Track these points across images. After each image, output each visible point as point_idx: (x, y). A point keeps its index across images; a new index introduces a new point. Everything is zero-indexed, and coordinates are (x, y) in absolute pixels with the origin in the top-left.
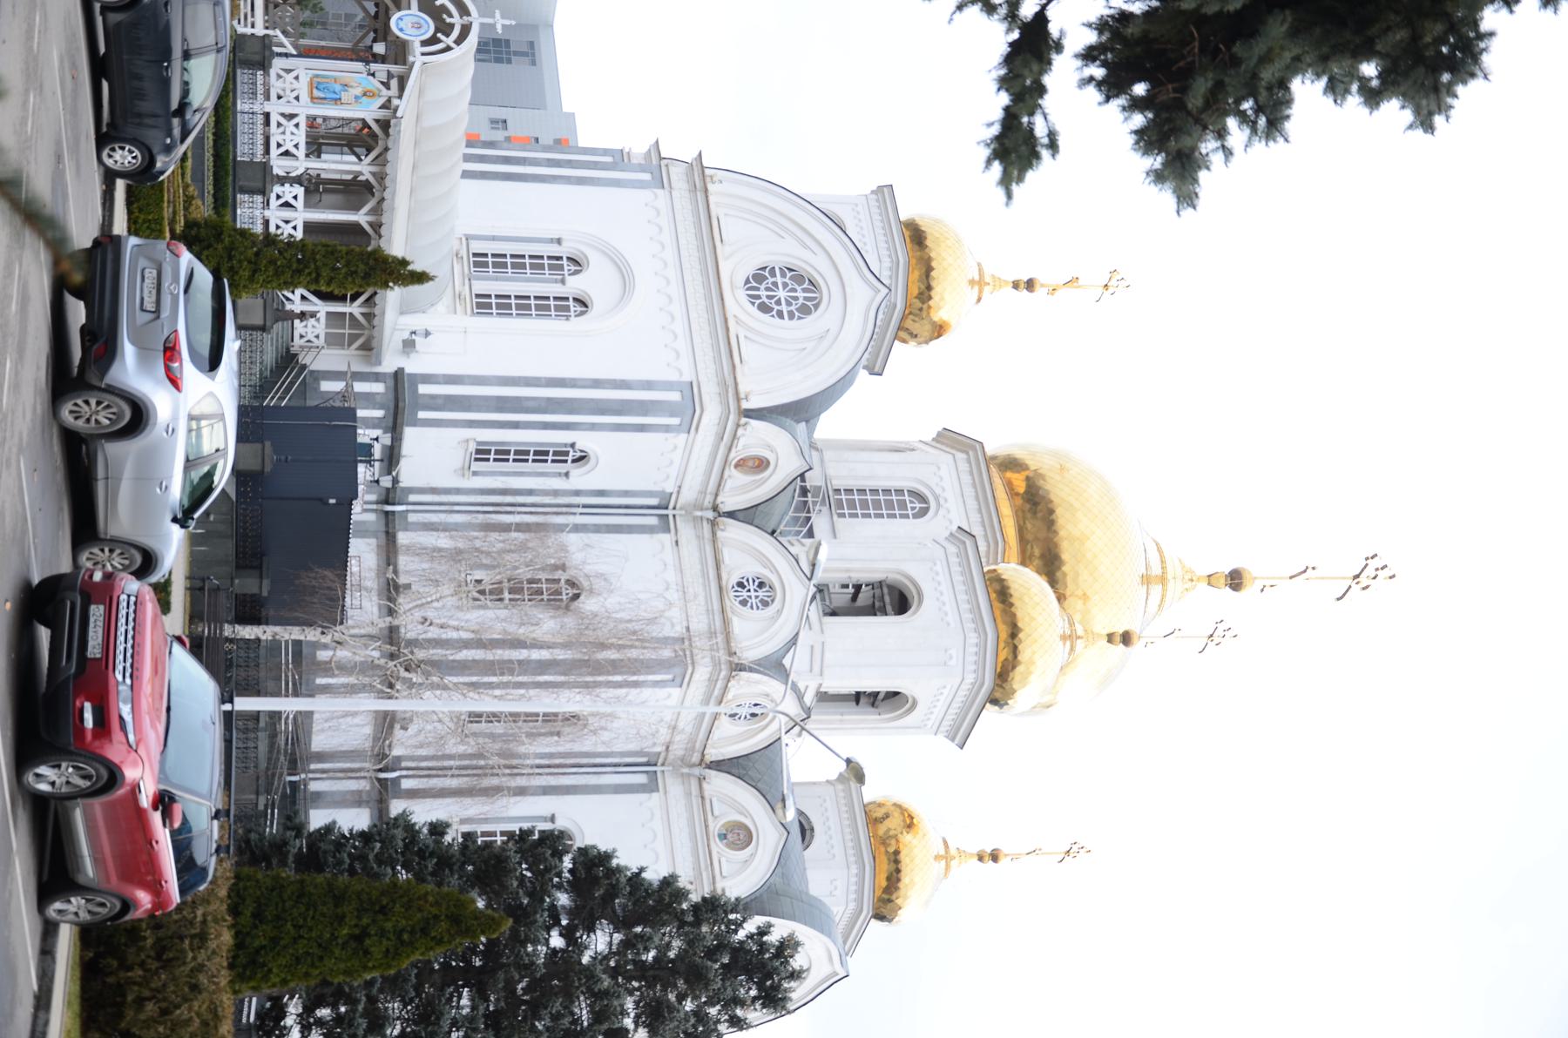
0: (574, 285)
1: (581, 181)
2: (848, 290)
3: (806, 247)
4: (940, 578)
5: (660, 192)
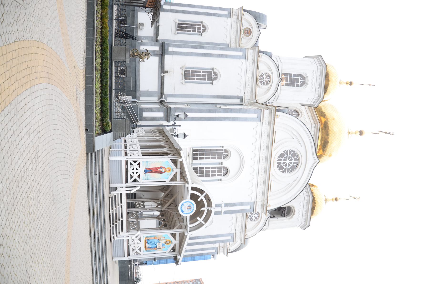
0: (226, 163)
1: (234, 119)
2: (307, 162)
3: (300, 143)
4: (301, 207)
5: (259, 123)
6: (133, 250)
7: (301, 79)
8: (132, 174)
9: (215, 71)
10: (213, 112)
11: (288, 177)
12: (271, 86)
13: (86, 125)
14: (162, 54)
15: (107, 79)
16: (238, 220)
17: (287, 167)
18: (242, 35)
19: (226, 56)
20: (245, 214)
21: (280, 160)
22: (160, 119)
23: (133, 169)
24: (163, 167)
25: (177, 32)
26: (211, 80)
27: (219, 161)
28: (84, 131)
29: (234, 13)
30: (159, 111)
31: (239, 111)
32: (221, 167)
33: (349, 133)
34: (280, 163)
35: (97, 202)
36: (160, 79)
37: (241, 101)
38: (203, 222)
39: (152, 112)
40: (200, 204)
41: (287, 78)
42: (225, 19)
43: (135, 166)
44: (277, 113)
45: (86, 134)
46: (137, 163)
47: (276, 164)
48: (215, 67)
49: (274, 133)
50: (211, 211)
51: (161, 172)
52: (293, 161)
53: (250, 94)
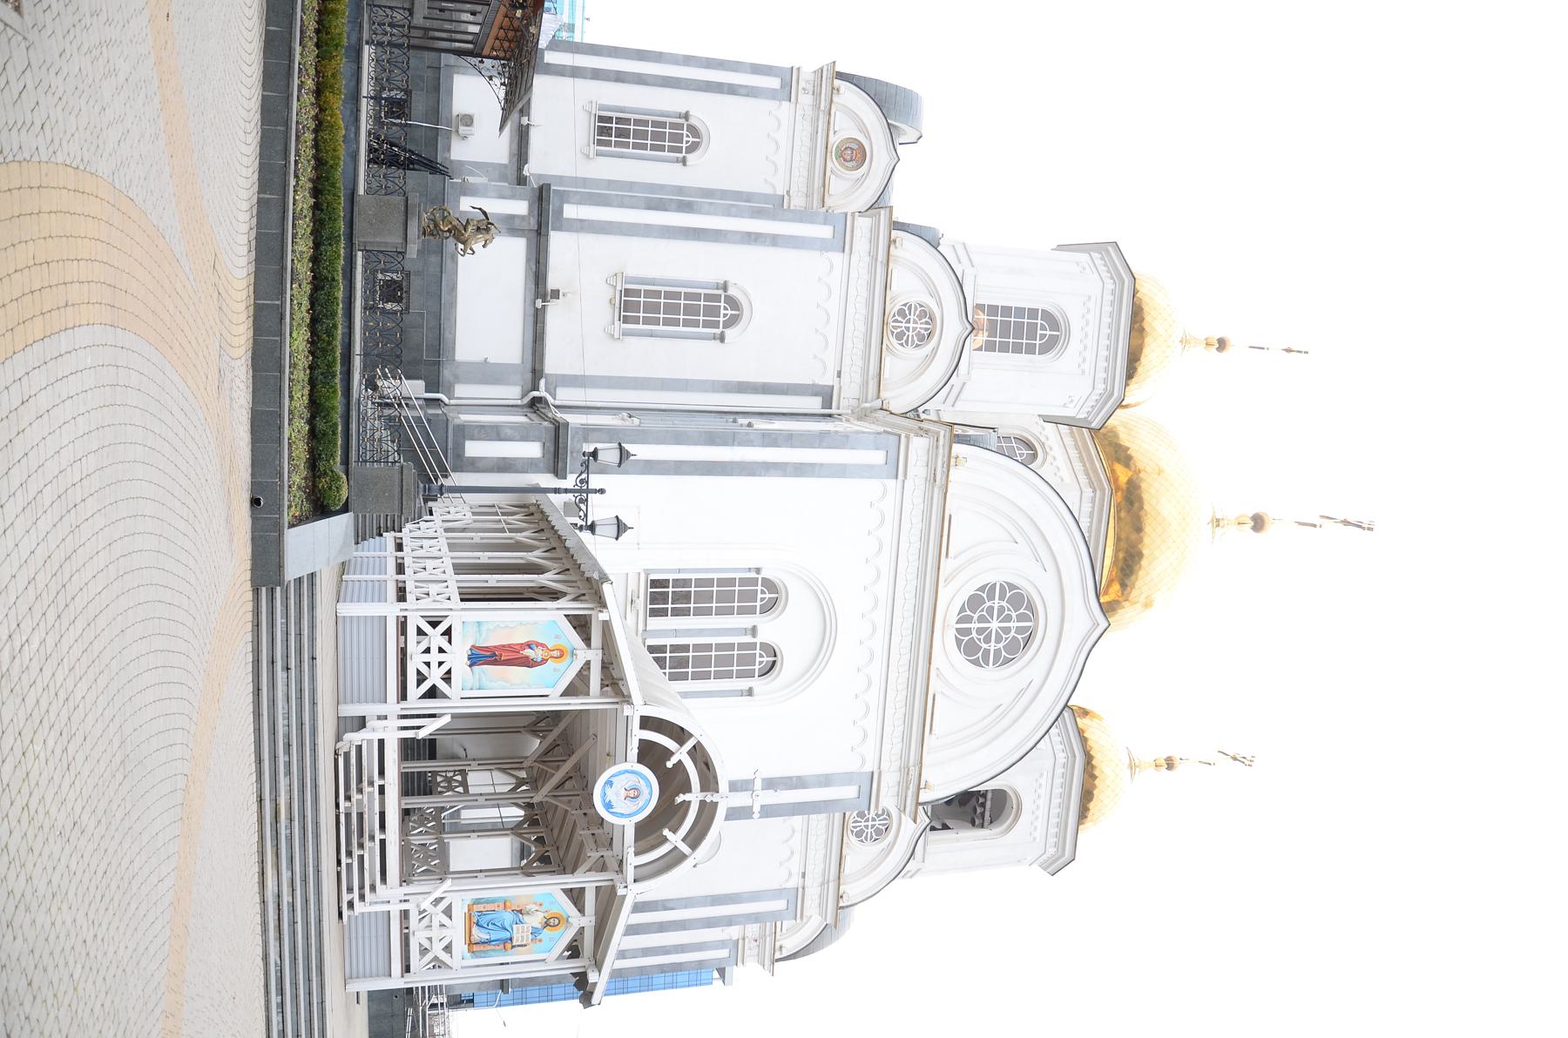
0: (770, 629)
1: (800, 470)
5: (891, 483)
6: (424, 951)
7: (1043, 328)
8: (424, 669)
9: (731, 292)
10: (725, 444)
11: (994, 683)
12: (935, 351)
13: (255, 485)
14: (538, 232)
15: (334, 314)
16: (812, 839)
17: (992, 646)
18: (833, 164)
19: (774, 240)
20: (838, 816)
21: (969, 619)
22: (528, 466)
23: (428, 651)
24: (538, 644)
25: (594, 148)
26: (715, 325)
27: (746, 621)
28: (248, 504)
29: (802, 84)
30: (523, 435)
31: (820, 440)
32: (752, 646)
33: (1217, 522)
34: (968, 631)
35: (289, 773)
36: (531, 319)
37: (827, 403)
38: (685, 848)
39: (499, 439)
40: (672, 781)
41: (992, 324)
42: (770, 105)
43: (435, 638)
44: (958, 448)
45: (254, 519)
46: (442, 628)
47: (952, 633)
48: (731, 280)
49: (945, 521)
50: (715, 805)
51: (528, 663)
52: (1013, 624)
53: (858, 379)
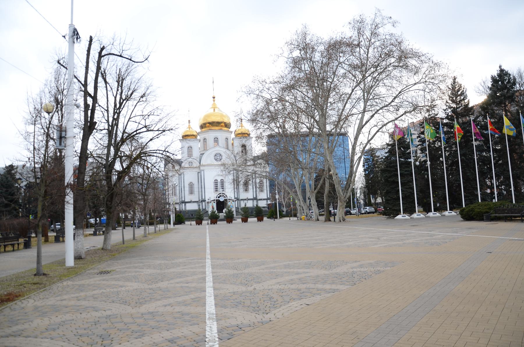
0: (219, 181)
14: (185, 203)
40: (220, 196)
